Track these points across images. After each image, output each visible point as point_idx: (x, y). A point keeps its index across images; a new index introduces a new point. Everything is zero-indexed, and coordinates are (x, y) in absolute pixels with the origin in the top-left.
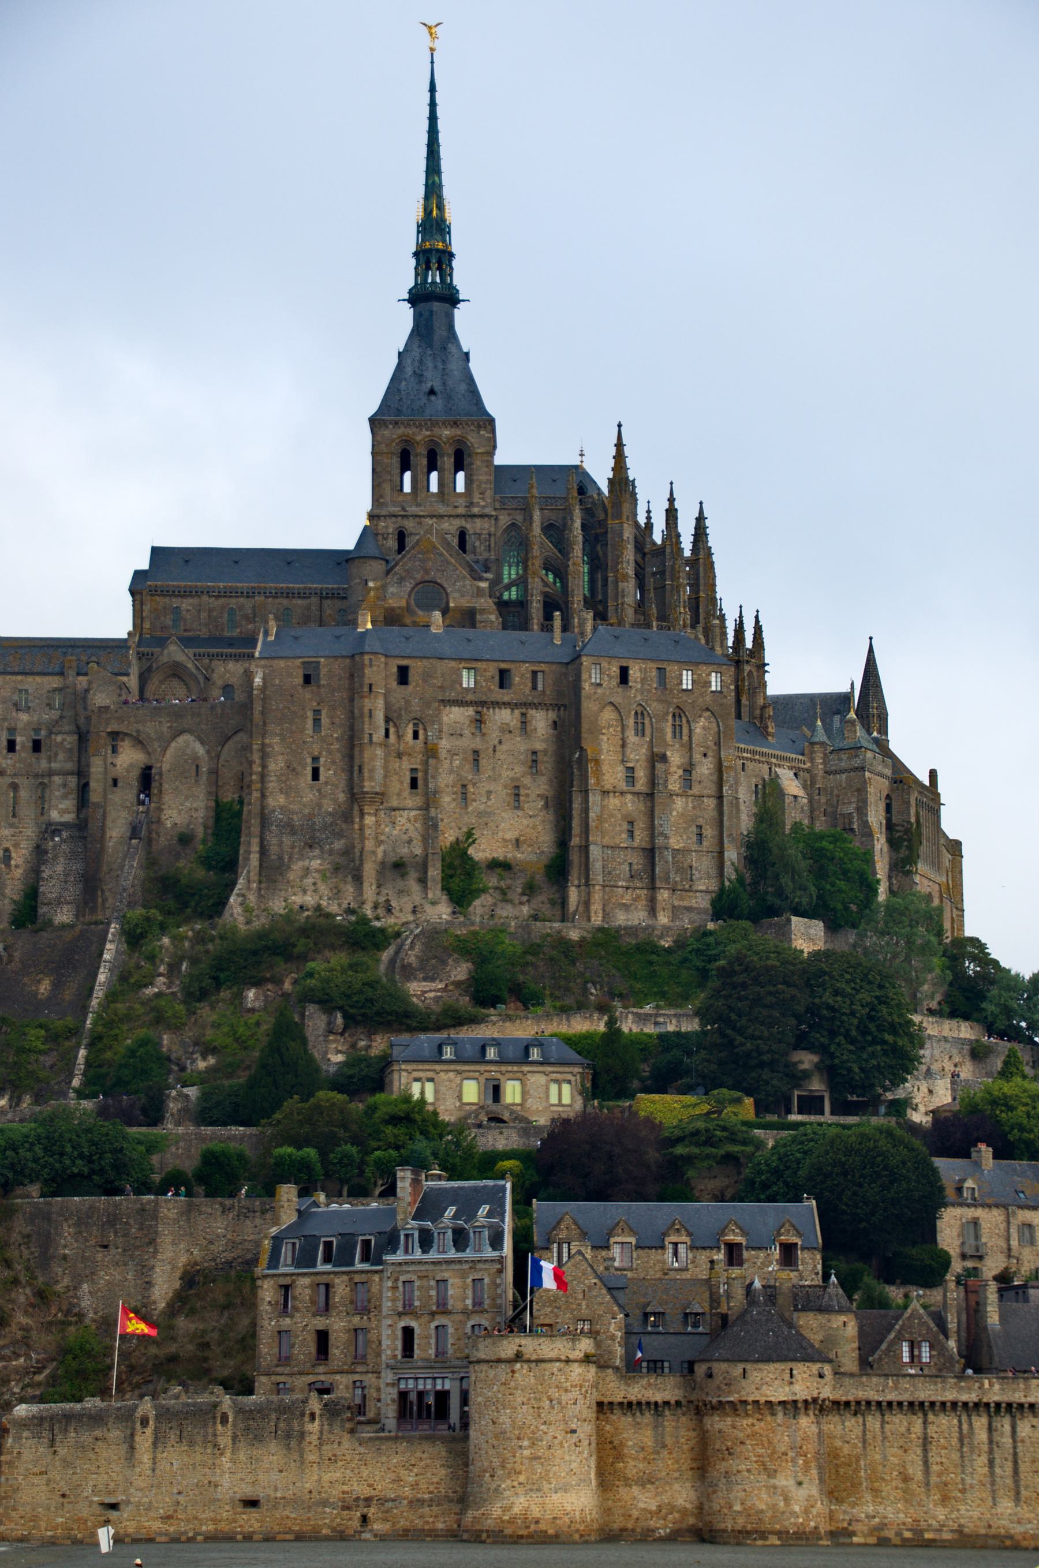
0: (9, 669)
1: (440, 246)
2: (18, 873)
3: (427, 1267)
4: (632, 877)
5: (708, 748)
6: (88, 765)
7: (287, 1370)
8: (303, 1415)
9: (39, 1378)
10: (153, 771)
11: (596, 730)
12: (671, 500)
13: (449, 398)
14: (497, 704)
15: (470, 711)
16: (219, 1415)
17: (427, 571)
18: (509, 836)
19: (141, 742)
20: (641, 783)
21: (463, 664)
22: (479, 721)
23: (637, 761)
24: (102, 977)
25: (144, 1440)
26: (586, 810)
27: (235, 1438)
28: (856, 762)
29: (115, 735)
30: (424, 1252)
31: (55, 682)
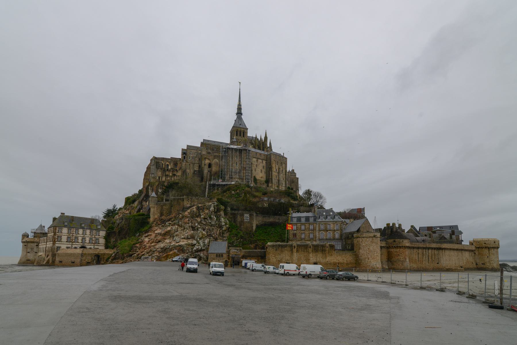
3: (326, 222)
4: (276, 183)
6: (202, 162)
7: (296, 240)
8: (325, 247)
9: (238, 241)
12: (270, 143)
14: (259, 159)
15: (256, 159)
16: (309, 246)
18: (261, 176)
19: (209, 159)
20: (277, 171)
22: (257, 161)
24: (207, 190)
25: (295, 250)
26: (272, 173)
27: (312, 251)
29: (205, 158)
30: (325, 220)
31: (196, 151)
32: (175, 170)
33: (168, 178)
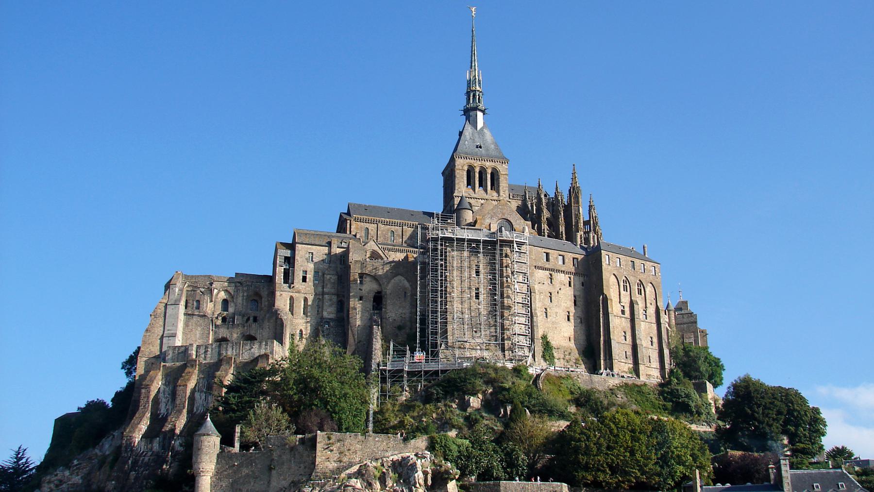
0: (304, 242)
1: (478, 88)
2: (304, 341)
4: (626, 358)
5: (652, 301)
10: (383, 293)
11: (608, 287)
13: (487, 150)
14: (558, 271)
15: (547, 272)
17: (503, 214)
18: (567, 335)
21: (544, 250)
22: (551, 279)
23: (625, 303)
28: (692, 320)
31: (325, 250)
32: (251, 319)
33: (229, 353)
